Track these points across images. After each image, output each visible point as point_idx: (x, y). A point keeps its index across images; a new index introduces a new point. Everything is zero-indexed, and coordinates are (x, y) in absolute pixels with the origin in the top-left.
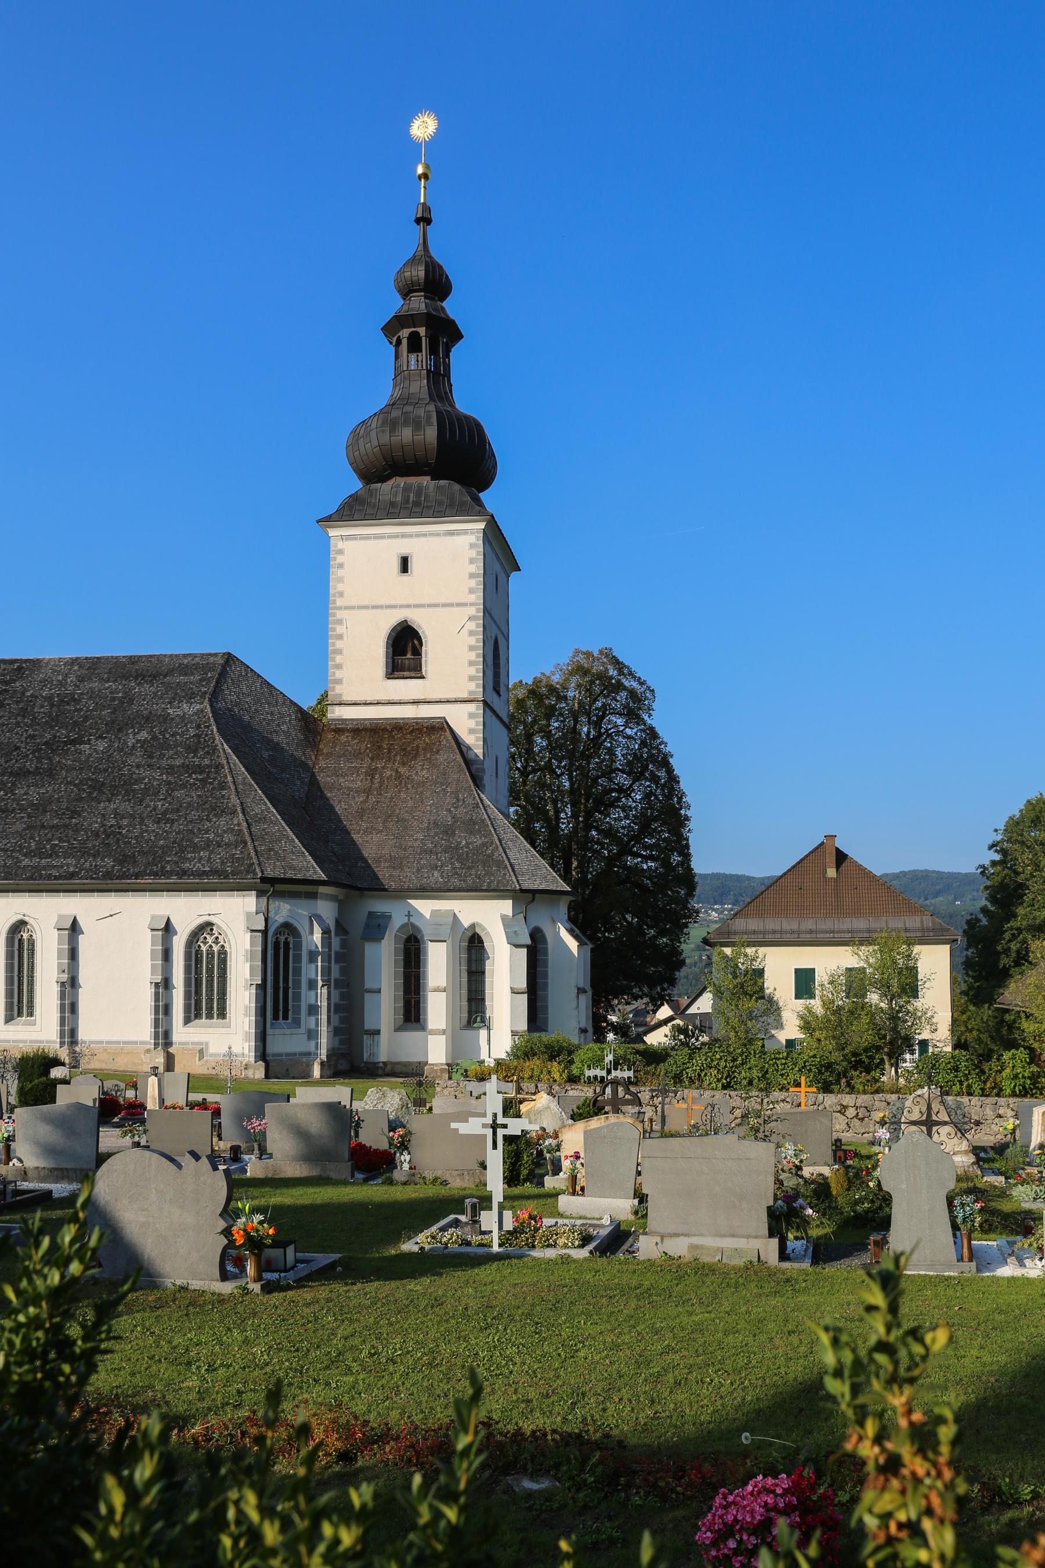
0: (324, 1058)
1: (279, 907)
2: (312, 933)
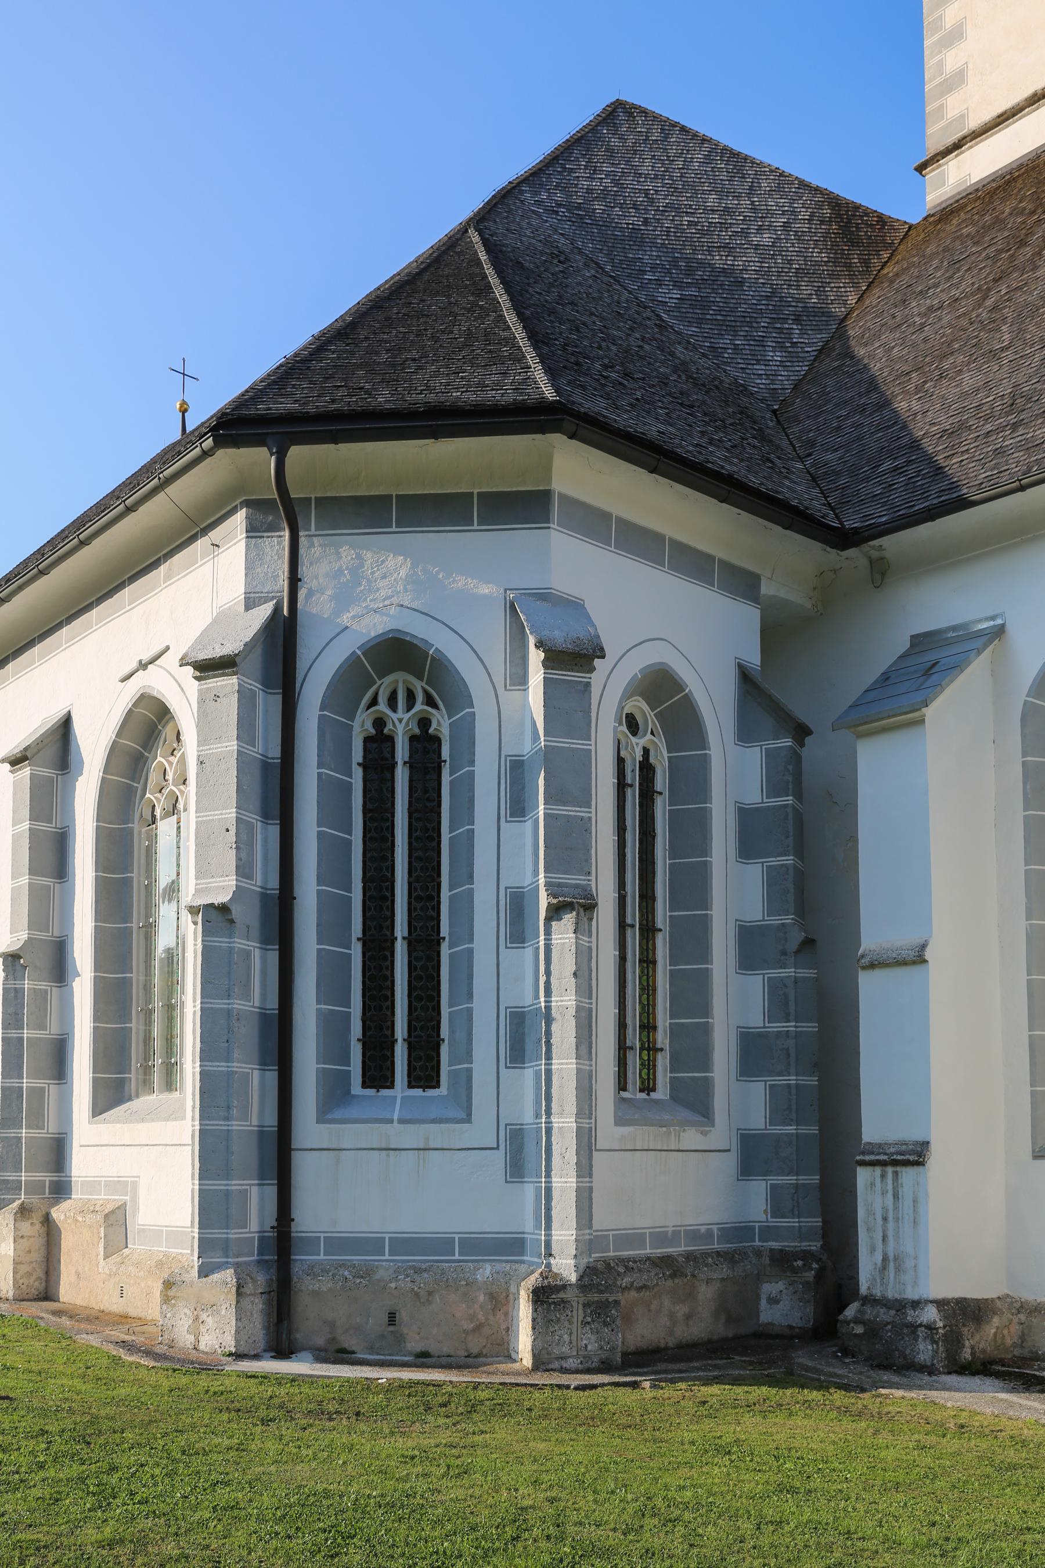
0: (566, 1267)
1: (356, 570)
2: (521, 680)
